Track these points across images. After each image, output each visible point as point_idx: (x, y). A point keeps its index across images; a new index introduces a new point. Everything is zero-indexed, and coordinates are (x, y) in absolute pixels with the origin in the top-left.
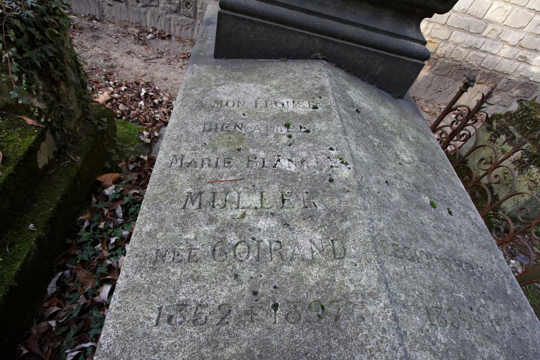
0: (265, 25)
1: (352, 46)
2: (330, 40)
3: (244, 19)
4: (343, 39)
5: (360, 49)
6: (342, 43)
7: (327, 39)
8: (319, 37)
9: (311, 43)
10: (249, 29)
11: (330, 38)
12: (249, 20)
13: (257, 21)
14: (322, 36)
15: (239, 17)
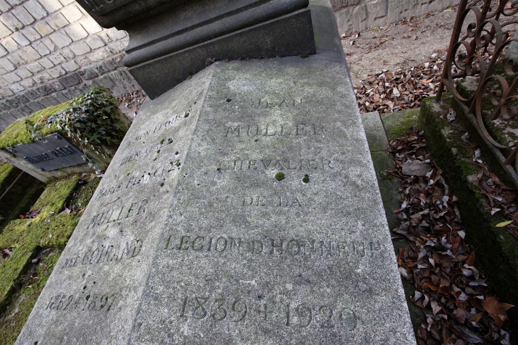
0: (158, 62)
1: (228, 37)
2: (207, 44)
3: (144, 65)
4: (216, 37)
5: (236, 35)
6: (218, 40)
7: (204, 45)
8: (198, 47)
9: (197, 55)
10: (152, 70)
11: (206, 43)
12: (147, 65)
13: (152, 62)
14: (200, 45)
15: (141, 66)
